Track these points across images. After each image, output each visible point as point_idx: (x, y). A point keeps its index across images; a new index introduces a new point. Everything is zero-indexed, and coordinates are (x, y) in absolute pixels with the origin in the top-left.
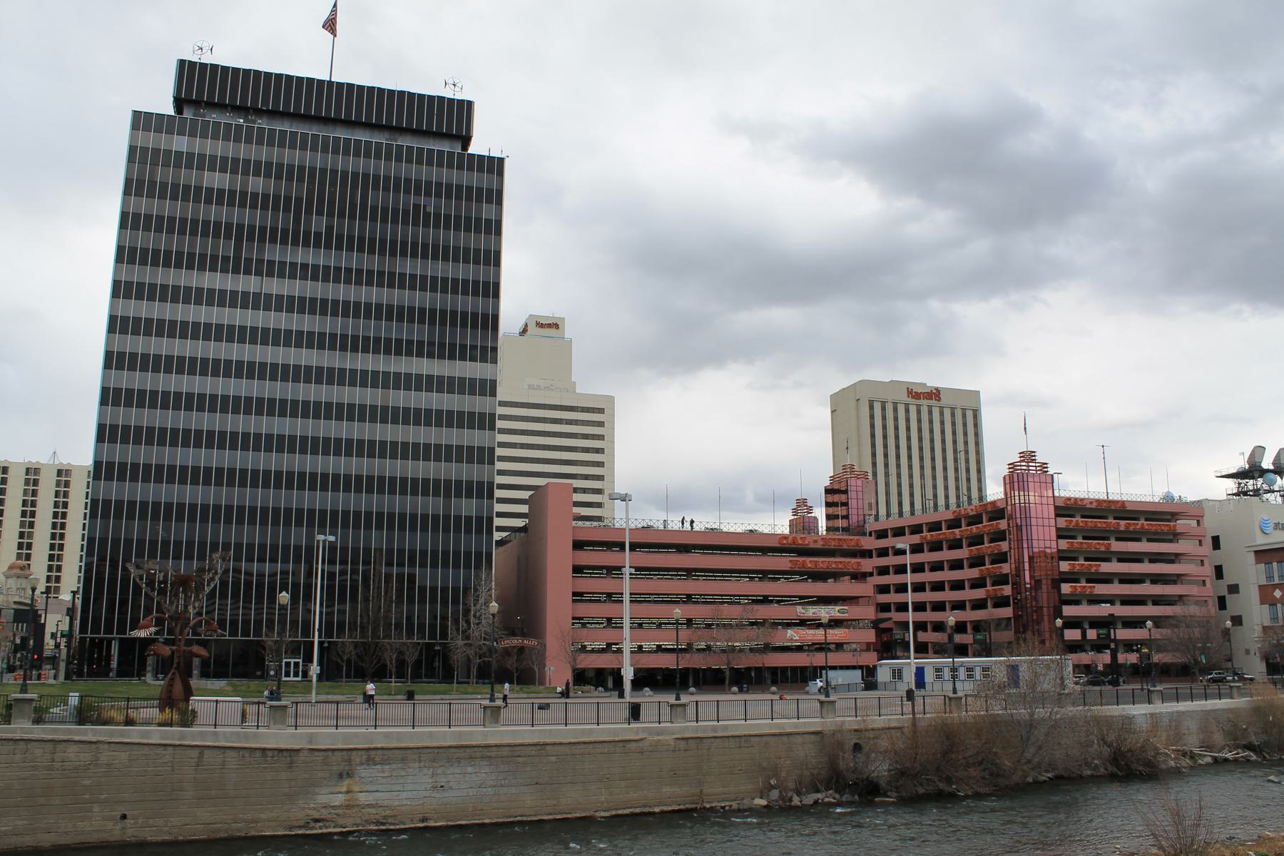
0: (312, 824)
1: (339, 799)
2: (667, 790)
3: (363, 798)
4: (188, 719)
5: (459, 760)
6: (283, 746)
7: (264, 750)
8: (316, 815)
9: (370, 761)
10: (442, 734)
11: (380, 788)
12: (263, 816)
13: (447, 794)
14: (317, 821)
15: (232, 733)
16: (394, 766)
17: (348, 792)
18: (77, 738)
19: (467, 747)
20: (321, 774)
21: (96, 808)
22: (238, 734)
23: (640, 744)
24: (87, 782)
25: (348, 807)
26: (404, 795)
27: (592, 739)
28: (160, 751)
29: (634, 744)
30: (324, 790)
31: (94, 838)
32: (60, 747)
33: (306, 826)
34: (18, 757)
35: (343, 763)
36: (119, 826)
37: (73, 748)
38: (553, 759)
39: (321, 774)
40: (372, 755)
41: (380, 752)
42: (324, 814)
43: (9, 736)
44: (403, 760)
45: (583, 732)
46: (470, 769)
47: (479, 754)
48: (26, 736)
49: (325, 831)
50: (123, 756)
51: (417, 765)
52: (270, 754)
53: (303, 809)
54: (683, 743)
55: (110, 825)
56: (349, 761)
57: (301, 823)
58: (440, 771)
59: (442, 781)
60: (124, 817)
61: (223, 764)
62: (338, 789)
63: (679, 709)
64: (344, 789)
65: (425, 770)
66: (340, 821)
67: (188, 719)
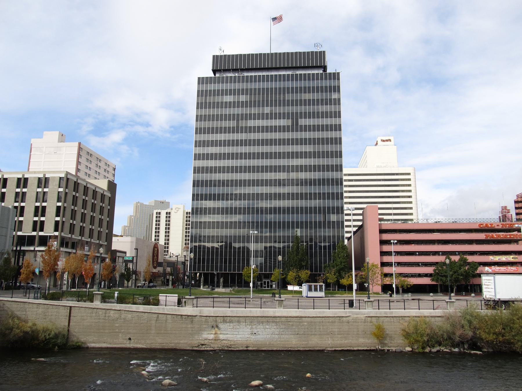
0: (201, 346)
1: (212, 337)
2: (361, 340)
3: (222, 337)
4: (157, 303)
5: (262, 323)
6: (189, 314)
7: (182, 315)
8: (203, 343)
9: (224, 321)
10: (256, 312)
11: (229, 333)
12: (181, 342)
13: (257, 337)
14: (203, 345)
15: (170, 309)
16: (235, 324)
17: (215, 334)
18: (113, 308)
19: (266, 317)
20: (205, 326)
21: (120, 335)
22: (172, 309)
23: (347, 318)
24: (117, 325)
25: (215, 340)
26: (239, 336)
27: (324, 316)
28: (143, 314)
29: (344, 318)
30: (205, 333)
31: (158, 346)
32: (108, 311)
33: (198, 346)
34: (94, 314)
35: (214, 323)
36: (128, 342)
37: (112, 312)
38: (305, 323)
39: (205, 326)
40: (225, 319)
41: (228, 318)
42: (206, 342)
43: (91, 307)
44: (239, 322)
45: (320, 312)
46: (267, 327)
47: (271, 320)
48: (97, 307)
49: (206, 349)
50: (129, 316)
51: (244, 324)
52: (184, 317)
53: (197, 340)
54: (369, 319)
55: (125, 341)
56: (216, 321)
57: (197, 345)
58: (254, 327)
59: (255, 331)
60: (130, 339)
61: (166, 321)
62: (211, 332)
63: (369, 303)
64: (214, 333)
65: (248, 326)
66: (212, 345)
67: (157, 303)
